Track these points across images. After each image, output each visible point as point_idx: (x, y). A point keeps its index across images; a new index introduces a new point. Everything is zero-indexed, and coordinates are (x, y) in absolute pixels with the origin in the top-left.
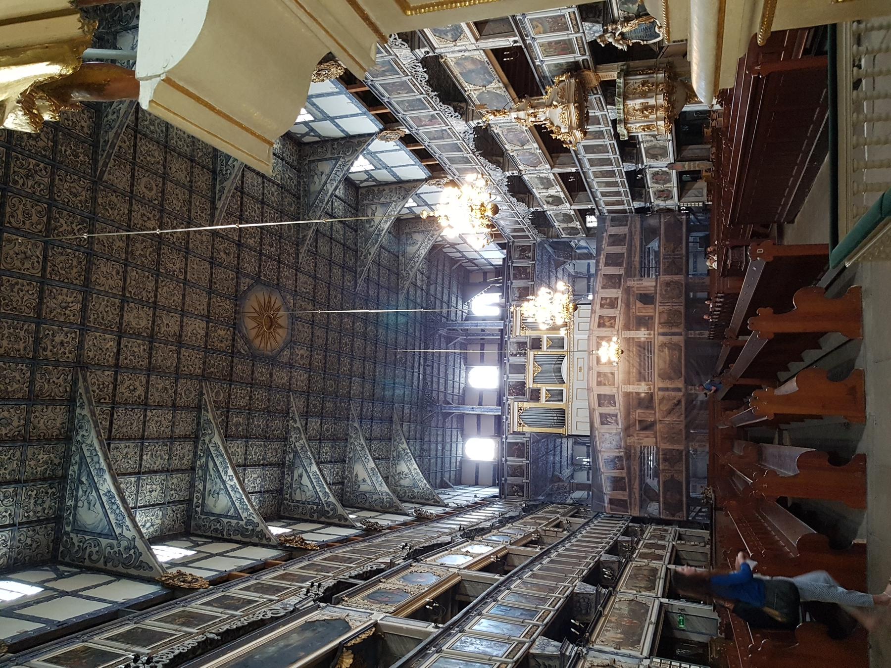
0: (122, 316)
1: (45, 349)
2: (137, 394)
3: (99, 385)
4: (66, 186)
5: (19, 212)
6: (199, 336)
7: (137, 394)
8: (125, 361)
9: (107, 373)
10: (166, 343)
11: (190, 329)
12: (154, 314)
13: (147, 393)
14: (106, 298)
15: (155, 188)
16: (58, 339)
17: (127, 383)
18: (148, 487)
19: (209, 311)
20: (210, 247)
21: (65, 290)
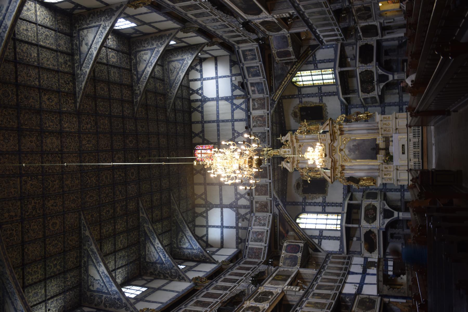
0: (61, 141)
2: (47, 97)
3: (68, 103)
4: (95, 198)
5: (109, 177)
7: (47, 97)
8: (56, 116)
9: (65, 109)
12: (42, 147)
13: (40, 97)
14: (71, 150)
15: (51, 227)
16: (89, 126)
17: (53, 103)
18: (29, 34)
21: (90, 149)
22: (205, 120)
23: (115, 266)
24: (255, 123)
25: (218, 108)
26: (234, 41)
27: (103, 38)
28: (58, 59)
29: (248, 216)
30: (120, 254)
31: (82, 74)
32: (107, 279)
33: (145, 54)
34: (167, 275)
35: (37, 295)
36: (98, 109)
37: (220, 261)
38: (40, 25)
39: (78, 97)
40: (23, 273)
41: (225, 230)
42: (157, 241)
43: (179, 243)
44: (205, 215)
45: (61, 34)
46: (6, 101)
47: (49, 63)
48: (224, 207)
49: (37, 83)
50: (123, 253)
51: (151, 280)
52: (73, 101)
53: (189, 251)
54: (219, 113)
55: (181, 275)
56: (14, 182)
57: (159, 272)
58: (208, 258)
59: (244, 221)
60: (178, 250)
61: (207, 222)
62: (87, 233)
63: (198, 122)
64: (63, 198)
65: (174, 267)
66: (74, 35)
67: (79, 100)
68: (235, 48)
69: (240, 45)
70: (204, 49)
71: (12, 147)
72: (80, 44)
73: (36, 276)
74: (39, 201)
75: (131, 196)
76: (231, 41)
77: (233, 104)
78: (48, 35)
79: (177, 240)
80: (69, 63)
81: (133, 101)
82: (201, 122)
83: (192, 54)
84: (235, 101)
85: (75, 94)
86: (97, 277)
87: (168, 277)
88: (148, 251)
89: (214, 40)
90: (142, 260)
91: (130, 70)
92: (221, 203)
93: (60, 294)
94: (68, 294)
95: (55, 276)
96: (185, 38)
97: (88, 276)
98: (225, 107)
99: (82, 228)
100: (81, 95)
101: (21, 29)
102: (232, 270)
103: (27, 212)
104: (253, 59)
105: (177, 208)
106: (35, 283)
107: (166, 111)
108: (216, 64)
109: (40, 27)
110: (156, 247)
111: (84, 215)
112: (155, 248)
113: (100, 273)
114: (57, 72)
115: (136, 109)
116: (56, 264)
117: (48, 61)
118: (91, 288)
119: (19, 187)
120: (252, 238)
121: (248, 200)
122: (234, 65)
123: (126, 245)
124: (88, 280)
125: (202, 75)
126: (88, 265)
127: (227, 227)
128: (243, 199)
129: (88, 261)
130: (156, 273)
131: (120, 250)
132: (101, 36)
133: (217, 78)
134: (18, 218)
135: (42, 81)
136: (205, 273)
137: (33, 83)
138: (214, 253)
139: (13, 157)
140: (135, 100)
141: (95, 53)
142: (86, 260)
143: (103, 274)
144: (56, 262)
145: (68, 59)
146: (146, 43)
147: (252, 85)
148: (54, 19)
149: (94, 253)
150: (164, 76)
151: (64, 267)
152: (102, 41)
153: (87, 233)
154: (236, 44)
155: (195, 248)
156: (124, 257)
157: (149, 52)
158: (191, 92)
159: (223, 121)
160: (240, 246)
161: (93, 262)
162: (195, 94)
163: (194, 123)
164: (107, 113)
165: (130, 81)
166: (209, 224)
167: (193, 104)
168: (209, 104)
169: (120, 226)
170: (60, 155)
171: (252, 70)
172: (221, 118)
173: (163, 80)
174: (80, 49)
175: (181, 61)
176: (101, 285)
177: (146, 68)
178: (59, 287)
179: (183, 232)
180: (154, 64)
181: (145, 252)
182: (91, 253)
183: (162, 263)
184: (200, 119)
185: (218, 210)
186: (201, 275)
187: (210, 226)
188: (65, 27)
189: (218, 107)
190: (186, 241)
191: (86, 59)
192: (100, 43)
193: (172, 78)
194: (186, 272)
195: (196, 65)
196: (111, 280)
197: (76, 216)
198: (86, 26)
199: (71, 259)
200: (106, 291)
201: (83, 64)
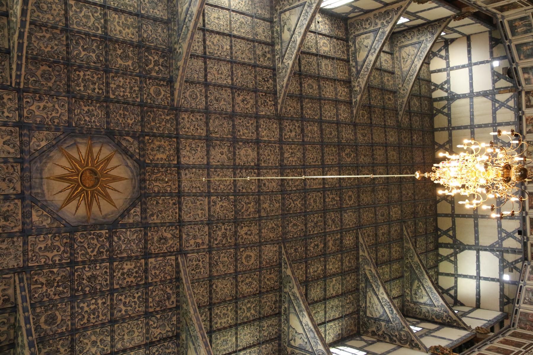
0: (258, 153)
1: (299, 127)
2: (241, 98)
3: (267, 105)
4: (300, 227)
5: (318, 201)
6: (188, 148)
7: (241, 98)
8: (252, 122)
9: (263, 113)
10: (222, 140)
11: (199, 154)
12: (235, 160)
13: (233, 98)
14: (270, 165)
15: (244, 261)
16: (293, 134)
17: (249, 106)
18: (221, 23)
19: (179, 174)
20: (184, 236)
21: (294, 164)
22: (453, 125)
23: (325, 318)
24: (530, 128)
25: (473, 108)
26: (495, 8)
27: (308, 19)
28: (255, 51)
29: (519, 265)
30: (332, 303)
31: (283, 68)
32: (311, 333)
33: (367, 38)
34: (395, 338)
35: (227, 343)
36: (304, 112)
37: (473, 327)
38: (233, 11)
39: (280, 97)
40: (211, 314)
41: (482, 282)
42: (382, 290)
43: (414, 296)
44: (452, 258)
45: (258, 20)
46: (193, 105)
47: (244, 56)
48: (481, 250)
49: (230, 81)
50: (336, 302)
51: (373, 343)
52: (273, 103)
53: (428, 308)
54: (473, 115)
55: (413, 341)
56: (202, 202)
57: (384, 332)
58: (455, 321)
59: (512, 271)
60: (412, 305)
61: (456, 269)
62: (289, 272)
63: (443, 129)
64: (260, 225)
65: (404, 327)
66: (275, 20)
67: (280, 101)
68: (497, 18)
69: (505, 14)
70: (450, 25)
71: (200, 160)
72: (282, 31)
73: (225, 320)
74: (230, 227)
75: (348, 227)
76: (490, 8)
77: (494, 101)
78: (243, 23)
79: (411, 291)
80: (269, 56)
81: (351, 100)
82: (448, 129)
83: (433, 34)
84: (498, 97)
85: (275, 93)
86: (300, 330)
87: (395, 341)
88: (370, 302)
89: (464, 10)
90: (361, 313)
91: (348, 61)
92: (477, 244)
93: (254, 346)
94: (264, 346)
95: (248, 322)
96: (421, 11)
97: (289, 327)
98: (483, 106)
99: (283, 264)
100: (282, 95)
101: (212, 17)
102: (491, 342)
103: (216, 239)
104: (526, 32)
105: (412, 248)
106: (225, 328)
107: (397, 114)
108: (469, 46)
109: (234, 13)
110: (380, 298)
111: (285, 248)
112: (378, 299)
113: (304, 325)
114: (255, 66)
115: (355, 112)
116: (250, 307)
117: (243, 54)
118: (292, 342)
119: (207, 208)
120: (525, 299)
121: (519, 241)
122: (496, 44)
123: (340, 292)
124: (289, 332)
125: (448, 63)
126: (289, 313)
127: (486, 279)
128: (510, 239)
129: (289, 307)
130: (380, 333)
131: (332, 297)
132: (305, 17)
133: (470, 65)
134: (205, 247)
135: (235, 79)
136: (451, 342)
137: (225, 82)
138: (465, 314)
139: (201, 171)
140: (354, 100)
141: (299, 40)
142: (286, 306)
143: (307, 327)
144: (249, 305)
145: (267, 50)
146: (367, 23)
147: (525, 70)
148: (250, 3)
149: (296, 298)
150: (394, 67)
151: (260, 313)
152: (307, 23)
153: (289, 272)
154: (498, 12)
155: (436, 304)
156: (337, 307)
157: (372, 35)
158: (433, 87)
159: (480, 126)
160: (506, 308)
161: (295, 310)
162: (439, 90)
163: (437, 130)
164: (316, 118)
165: (347, 75)
166: (459, 273)
167: (436, 105)
168: (458, 102)
169: (332, 266)
170: (256, 171)
171: (525, 48)
172: (477, 122)
173: (393, 73)
174: (281, 36)
175: (416, 45)
176: (304, 341)
177: (367, 56)
178: (253, 337)
179: (419, 280)
180: (378, 50)
181: (366, 303)
182: (292, 298)
183: (388, 321)
184: (446, 125)
185: (474, 253)
186: (444, 343)
187: (460, 276)
188: (264, 11)
189: (472, 107)
190: (424, 293)
191: (289, 49)
192: (305, 26)
193: (405, 69)
194: (421, 336)
195: (440, 50)
196: (316, 335)
197: (275, 249)
198: (288, 7)
199: (268, 304)
200: (310, 350)
201: (285, 55)
